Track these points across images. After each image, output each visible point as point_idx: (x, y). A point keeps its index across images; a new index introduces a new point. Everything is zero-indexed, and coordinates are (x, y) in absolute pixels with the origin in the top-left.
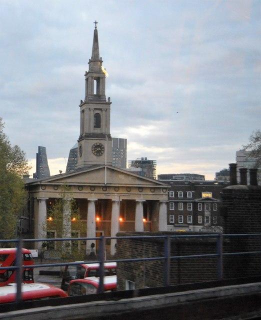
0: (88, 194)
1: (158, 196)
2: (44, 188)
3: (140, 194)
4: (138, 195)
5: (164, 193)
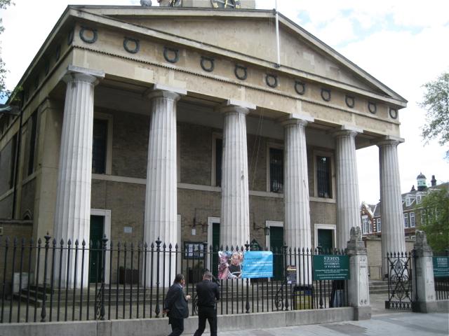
0: (230, 87)
1: (383, 125)
2: (88, 36)
3: (351, 113)
4: (347, 115)
5: (392, 120)
